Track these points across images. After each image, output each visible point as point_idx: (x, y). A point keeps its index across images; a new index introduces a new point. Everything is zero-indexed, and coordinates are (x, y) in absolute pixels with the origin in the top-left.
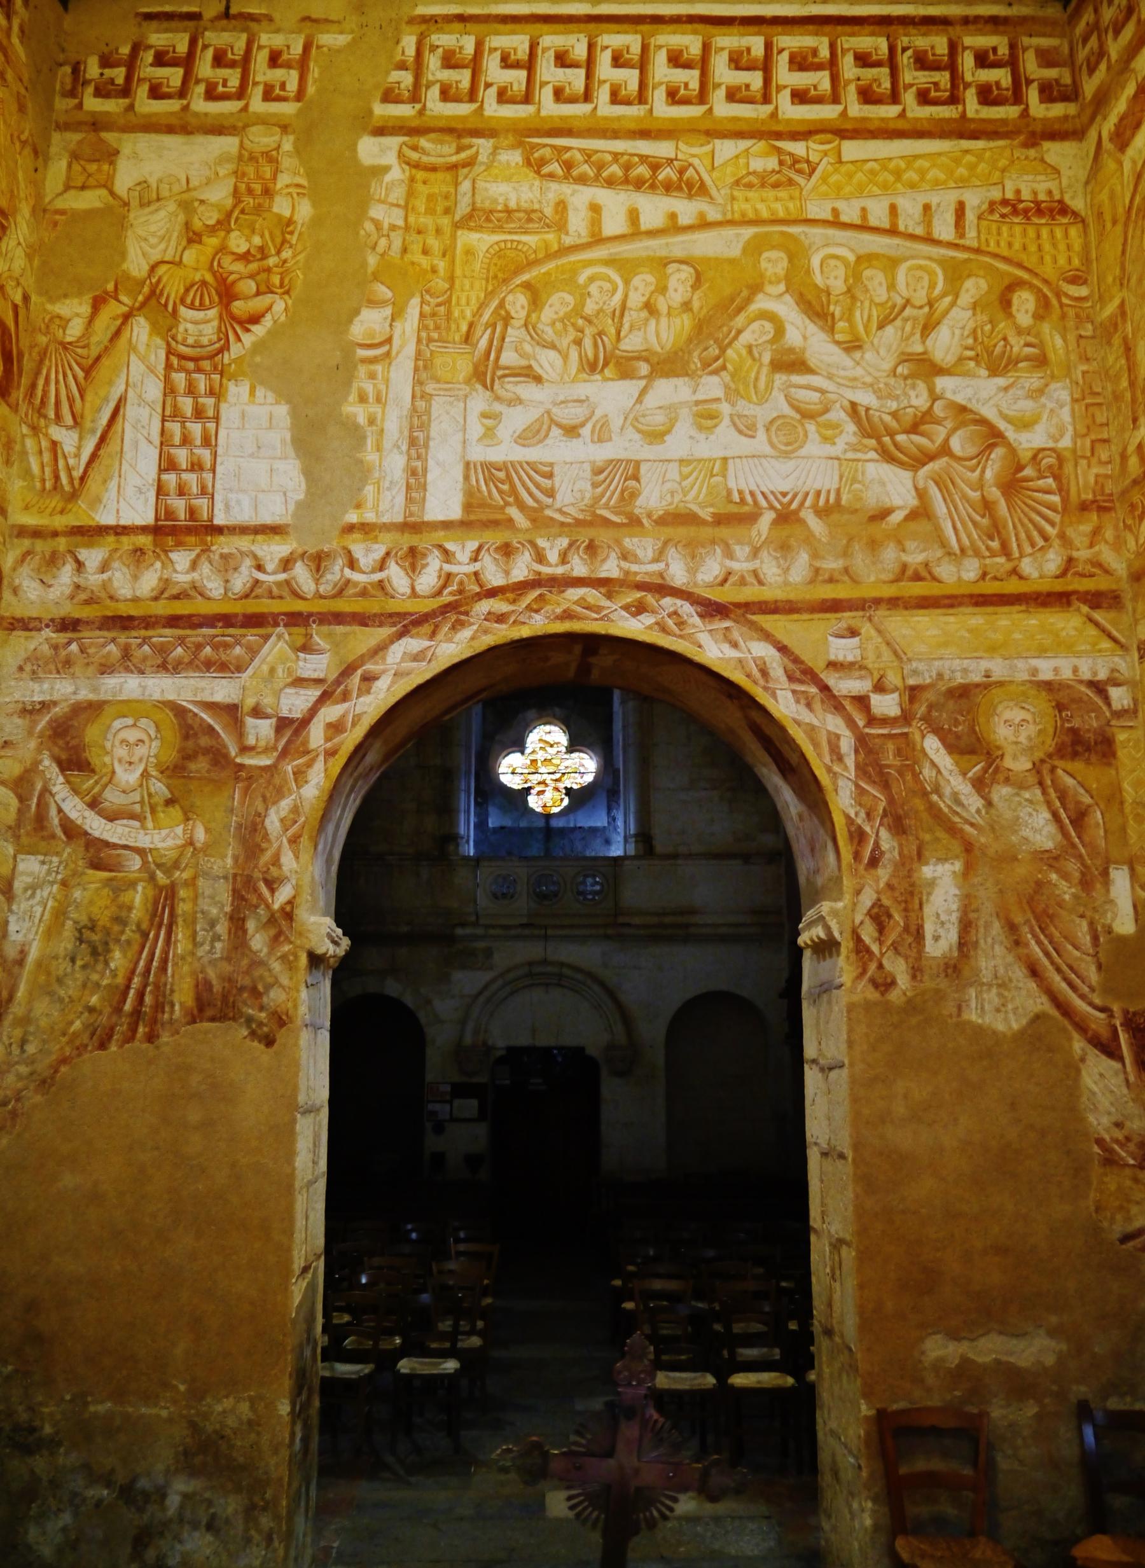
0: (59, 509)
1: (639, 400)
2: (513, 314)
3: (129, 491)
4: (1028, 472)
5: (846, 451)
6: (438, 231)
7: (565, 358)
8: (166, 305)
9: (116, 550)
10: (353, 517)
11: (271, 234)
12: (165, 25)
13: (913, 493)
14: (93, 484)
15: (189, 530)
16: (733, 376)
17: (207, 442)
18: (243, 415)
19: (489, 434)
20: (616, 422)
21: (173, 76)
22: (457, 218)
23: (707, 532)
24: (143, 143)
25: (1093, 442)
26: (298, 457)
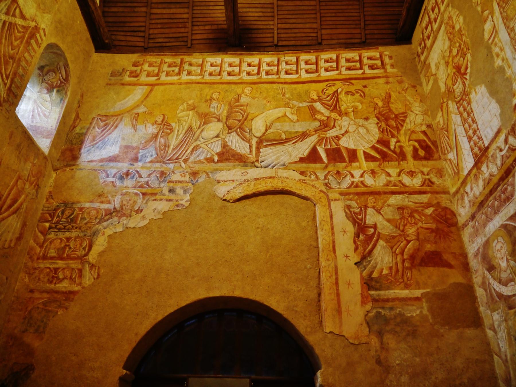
17: (474, 121)
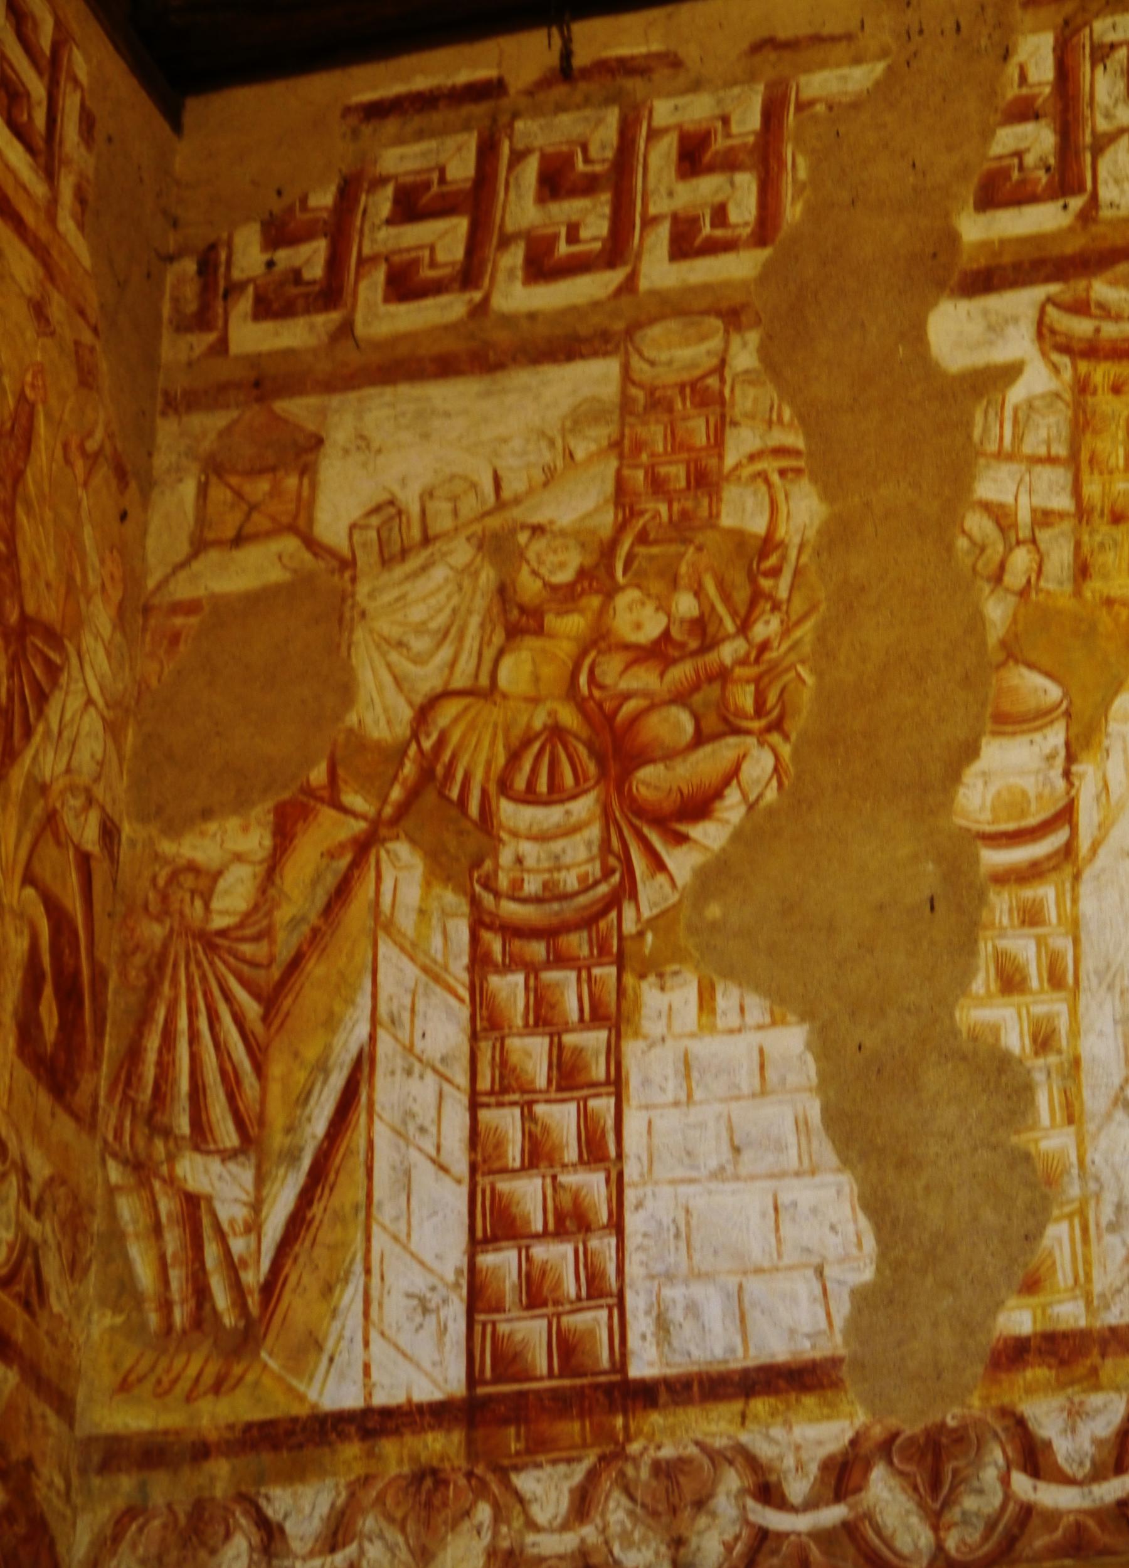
0: (208, 1379)
3: (394, 1308)
8: (462, 802)
9: (366, 1480)
10: (1019, 1319)
11: (721, 585)
12: (417, 122)
14: (298, 1305)
15: (562, 1404)
17: (598, 1148)
18: (687, 1064)
21: (447, 238)
24: (381, 409)
26: (846, 1162)
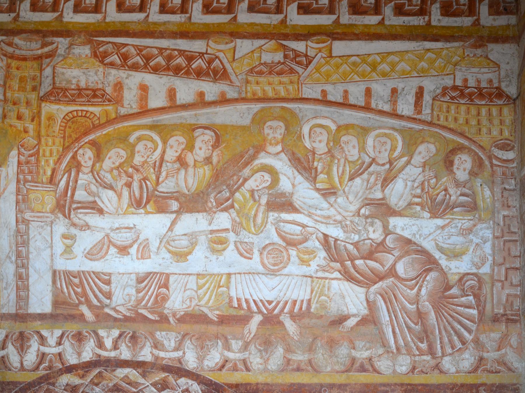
1: (171, 229)
2: (83, 163)
4: (454, 291)
5: (317, 271)
6: (28, 103)
7: (120, 196)
13: (365, 304)
16: (238, 213)
19: (68, 250)
20: (154, 244)
22: (42, 94)
23: (213, 329)
25: (507, 269)
